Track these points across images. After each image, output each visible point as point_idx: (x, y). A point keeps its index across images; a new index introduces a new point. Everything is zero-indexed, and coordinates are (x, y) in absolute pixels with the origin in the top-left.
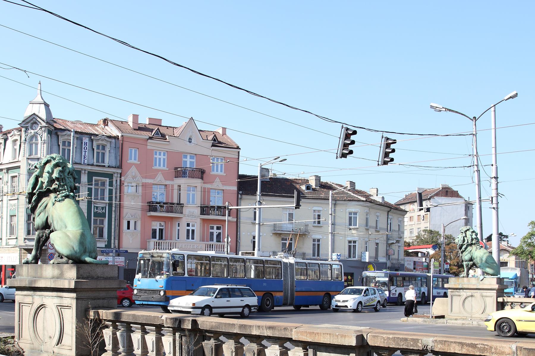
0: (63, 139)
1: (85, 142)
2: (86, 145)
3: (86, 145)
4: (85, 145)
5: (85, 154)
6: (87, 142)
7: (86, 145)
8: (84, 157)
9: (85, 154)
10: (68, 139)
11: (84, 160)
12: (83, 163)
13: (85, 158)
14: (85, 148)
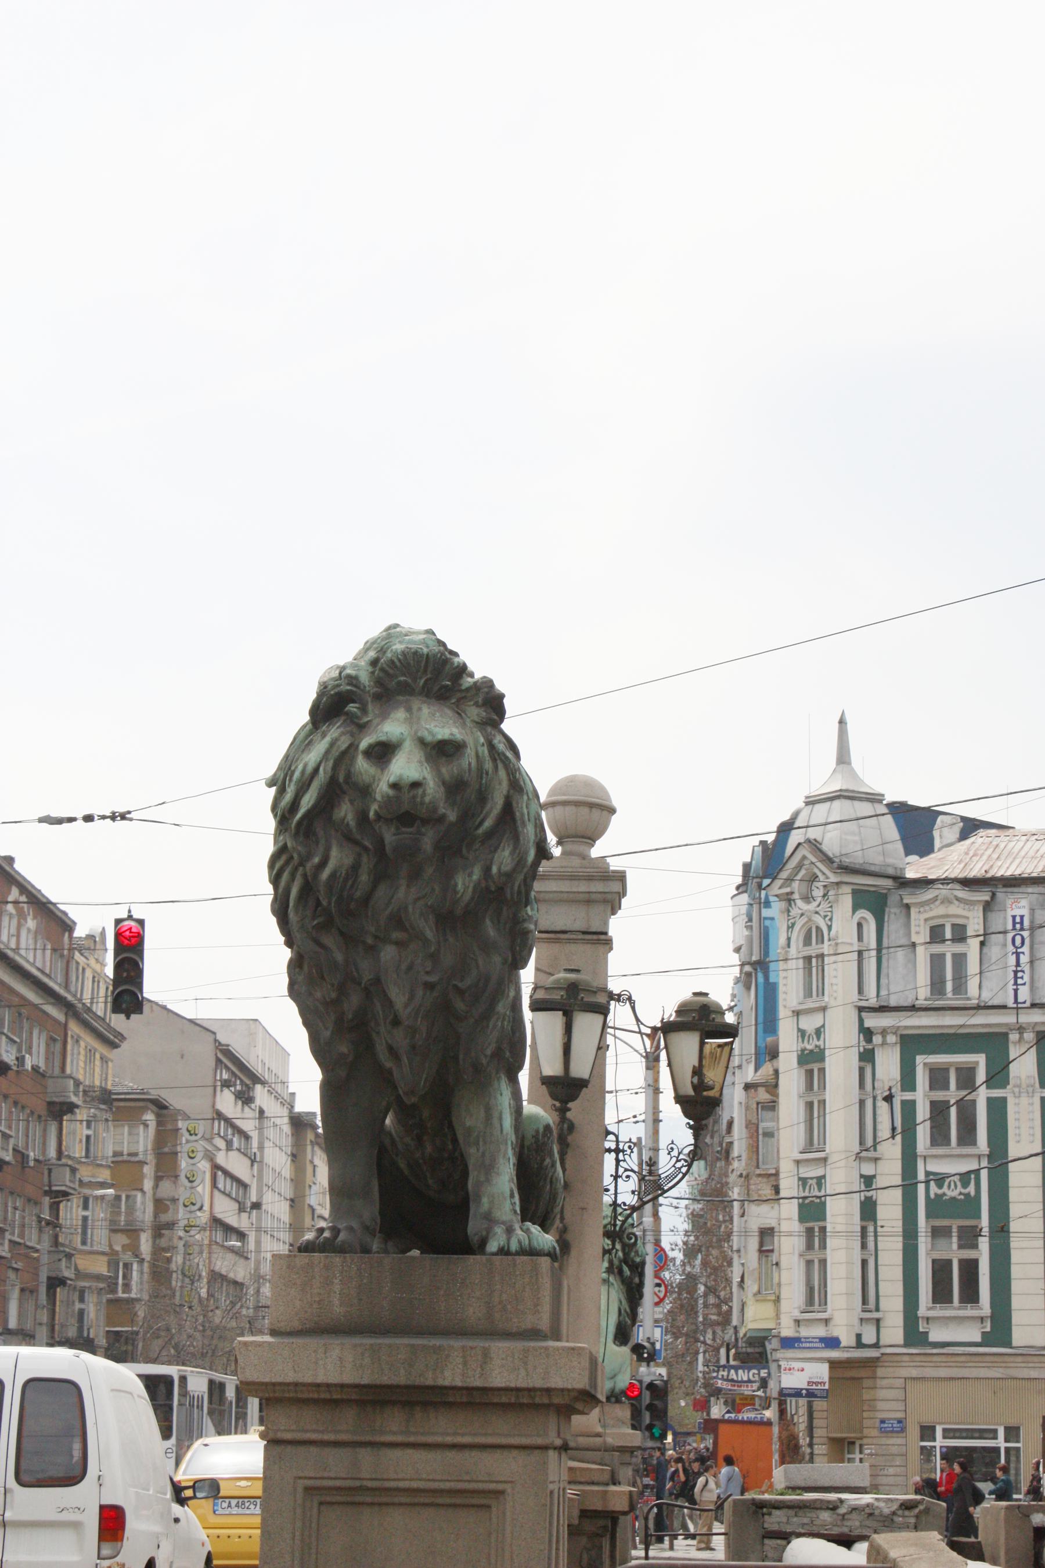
0: (926, 920)
1: (1014, 917)
2: (1018, 926)
5: (1018, 964)
6: (1022, 917)
8: (1016, 978)
9: (1018, 964)
10: (947, 916)
11: (1016, 991)
12: (1010, 1003)
13: (1020, 981)
14: (1018, 940)
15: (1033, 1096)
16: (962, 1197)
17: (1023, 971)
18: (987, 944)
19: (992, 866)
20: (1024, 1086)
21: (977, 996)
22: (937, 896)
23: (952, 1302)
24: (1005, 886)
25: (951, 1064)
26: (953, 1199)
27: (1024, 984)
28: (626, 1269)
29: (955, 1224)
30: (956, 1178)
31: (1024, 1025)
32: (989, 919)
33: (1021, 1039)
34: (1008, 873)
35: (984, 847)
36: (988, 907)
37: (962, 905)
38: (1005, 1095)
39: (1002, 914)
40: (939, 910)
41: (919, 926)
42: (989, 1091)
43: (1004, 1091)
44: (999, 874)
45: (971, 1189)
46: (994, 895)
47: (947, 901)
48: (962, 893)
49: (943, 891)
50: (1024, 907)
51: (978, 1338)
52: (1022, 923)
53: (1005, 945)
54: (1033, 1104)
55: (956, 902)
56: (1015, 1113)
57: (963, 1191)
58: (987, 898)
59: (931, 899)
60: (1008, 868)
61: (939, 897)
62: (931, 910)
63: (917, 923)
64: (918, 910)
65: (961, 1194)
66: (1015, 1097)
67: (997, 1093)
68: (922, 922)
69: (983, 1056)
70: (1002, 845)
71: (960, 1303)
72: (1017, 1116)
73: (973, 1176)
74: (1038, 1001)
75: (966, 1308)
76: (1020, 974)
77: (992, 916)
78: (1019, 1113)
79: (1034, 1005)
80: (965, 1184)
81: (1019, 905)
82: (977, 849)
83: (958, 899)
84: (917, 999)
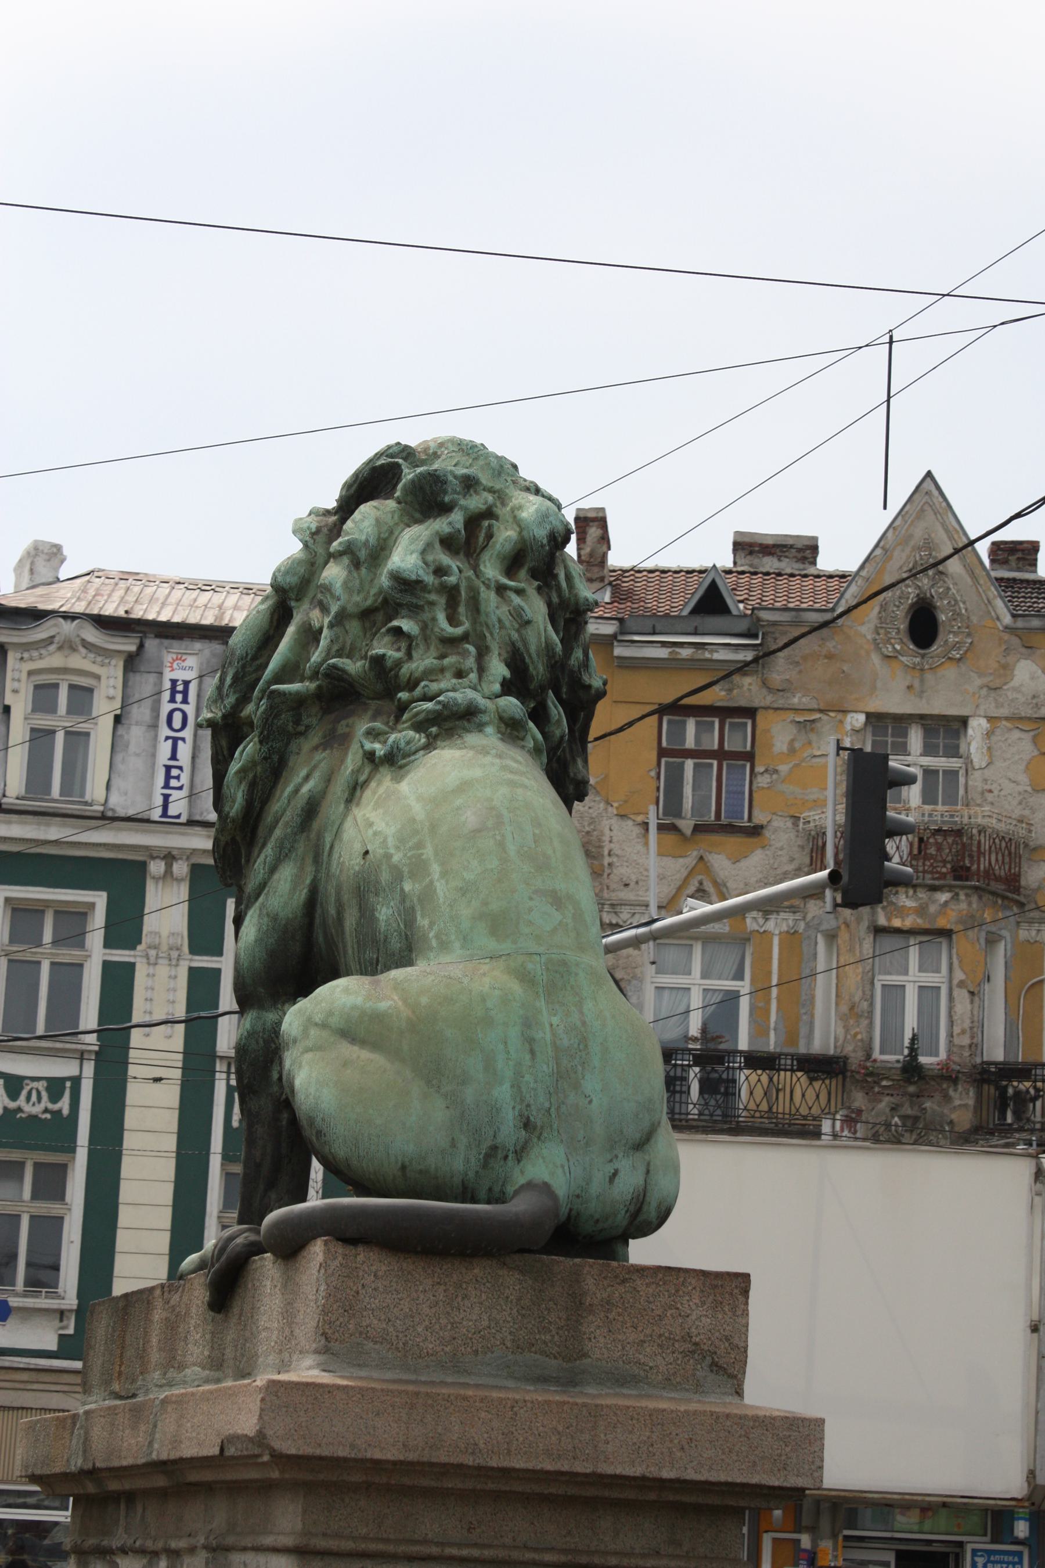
0: (30, 673)
1: (174, 682)
2: (179, 697)
3: (179, 697)
4: (172, 700)
5: (174, 757)
6: (186, 683)
7: (185, 701)
8: (168, 777)
9: (174, 757)
10: (65, 670)
11: (166, 797)
12: (156, 815)
13: (173, 783)
14: (177, 717)
15: (177, 965)
16: (48, 1116)
17: (180, 768)
18: (123, 721)
19: (132, 608)
20: (164, 947)
21: (103, 801)
22: (53, 637)
23: (13, 1284)
24: (159, 635)
25: (47, 903)
26: (33, 1118)
27: (180, 788)
28: (556, 711)
29: (30, 1160)
30: (41, 1085)
31: (175, 853)
32: (130, 683)
33: (168, 871)
34: (163, 618)
35: (110, 588)
36: (132, 663)
37: (92, 656)
38: (132, 960)
39: (152, 678)
40: (56, 660)
41: (19, 680)
42: (108, 951)
43: (132, 953)
44: (151, 616)
45: (64, 1105)
46: (141, 646)
47: (68, 646)
48: (92, 634)
49: (67, 628)
50: (191, 668)
51: (52, 1345)
52: (185, 693)
53: (154, 726)
54: (176, 977)
55: (83, 651)
56: (147, 988)
57: (50, 1106)
58: (133, 648)
59: (43, 640)
60: (159, 613)
61: (56, 639)
62: (41, 657)
63: (16, 675)
64: (18, 655)
65: (46, 1111)
66: (149, 964)
67: (120, 956)
68: (24, 676)
69: (104, 894)
70: (136, 589)
71: (25, 1285)
72: (149, 994)
73: (68, 1084)
74: (198, 818)
75: (36, 1295)
76: (174, 772)
77: (135, 679)
78: (153, 989)
79: (191, 823)
80: (55, 1097)
81: (185, 664)
82: (98, 589)
83: (85, 644)
84: (4, 796)
